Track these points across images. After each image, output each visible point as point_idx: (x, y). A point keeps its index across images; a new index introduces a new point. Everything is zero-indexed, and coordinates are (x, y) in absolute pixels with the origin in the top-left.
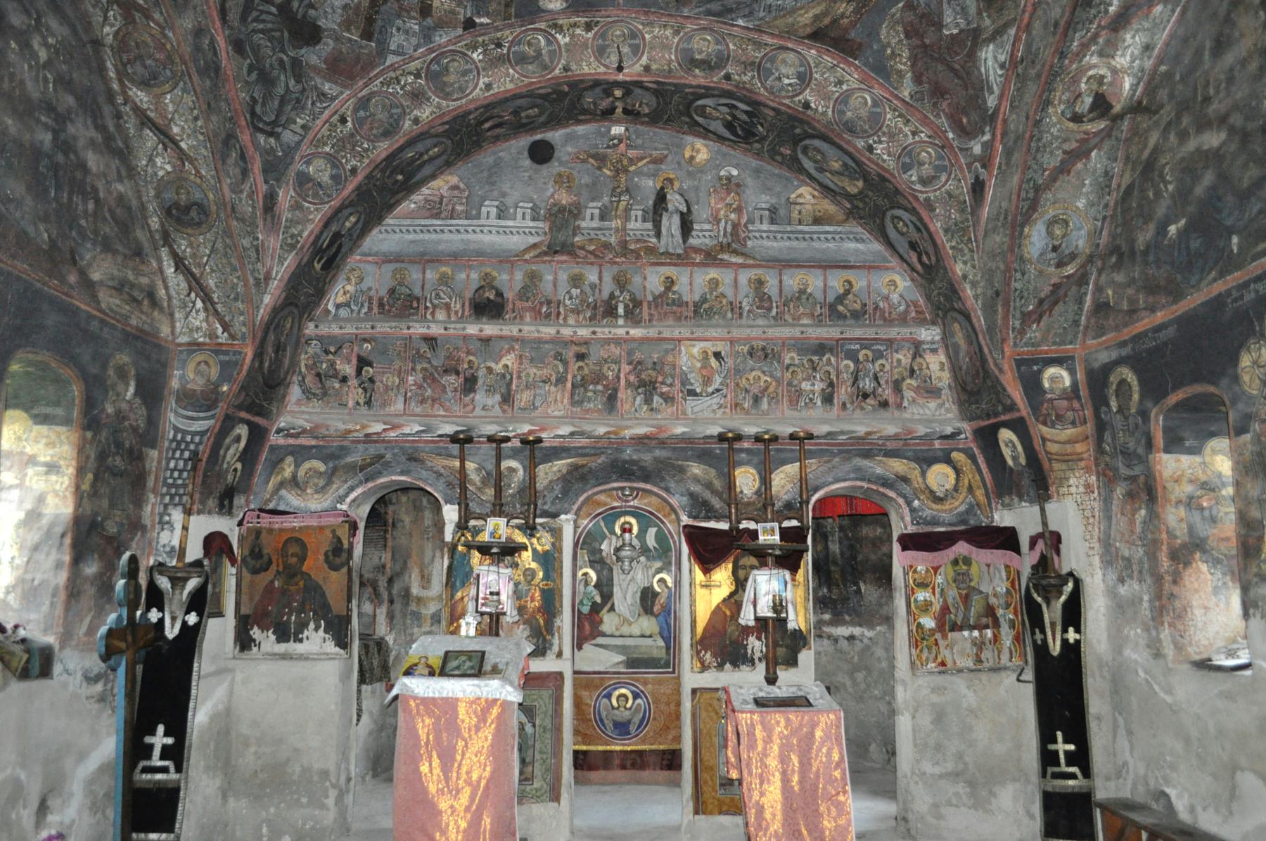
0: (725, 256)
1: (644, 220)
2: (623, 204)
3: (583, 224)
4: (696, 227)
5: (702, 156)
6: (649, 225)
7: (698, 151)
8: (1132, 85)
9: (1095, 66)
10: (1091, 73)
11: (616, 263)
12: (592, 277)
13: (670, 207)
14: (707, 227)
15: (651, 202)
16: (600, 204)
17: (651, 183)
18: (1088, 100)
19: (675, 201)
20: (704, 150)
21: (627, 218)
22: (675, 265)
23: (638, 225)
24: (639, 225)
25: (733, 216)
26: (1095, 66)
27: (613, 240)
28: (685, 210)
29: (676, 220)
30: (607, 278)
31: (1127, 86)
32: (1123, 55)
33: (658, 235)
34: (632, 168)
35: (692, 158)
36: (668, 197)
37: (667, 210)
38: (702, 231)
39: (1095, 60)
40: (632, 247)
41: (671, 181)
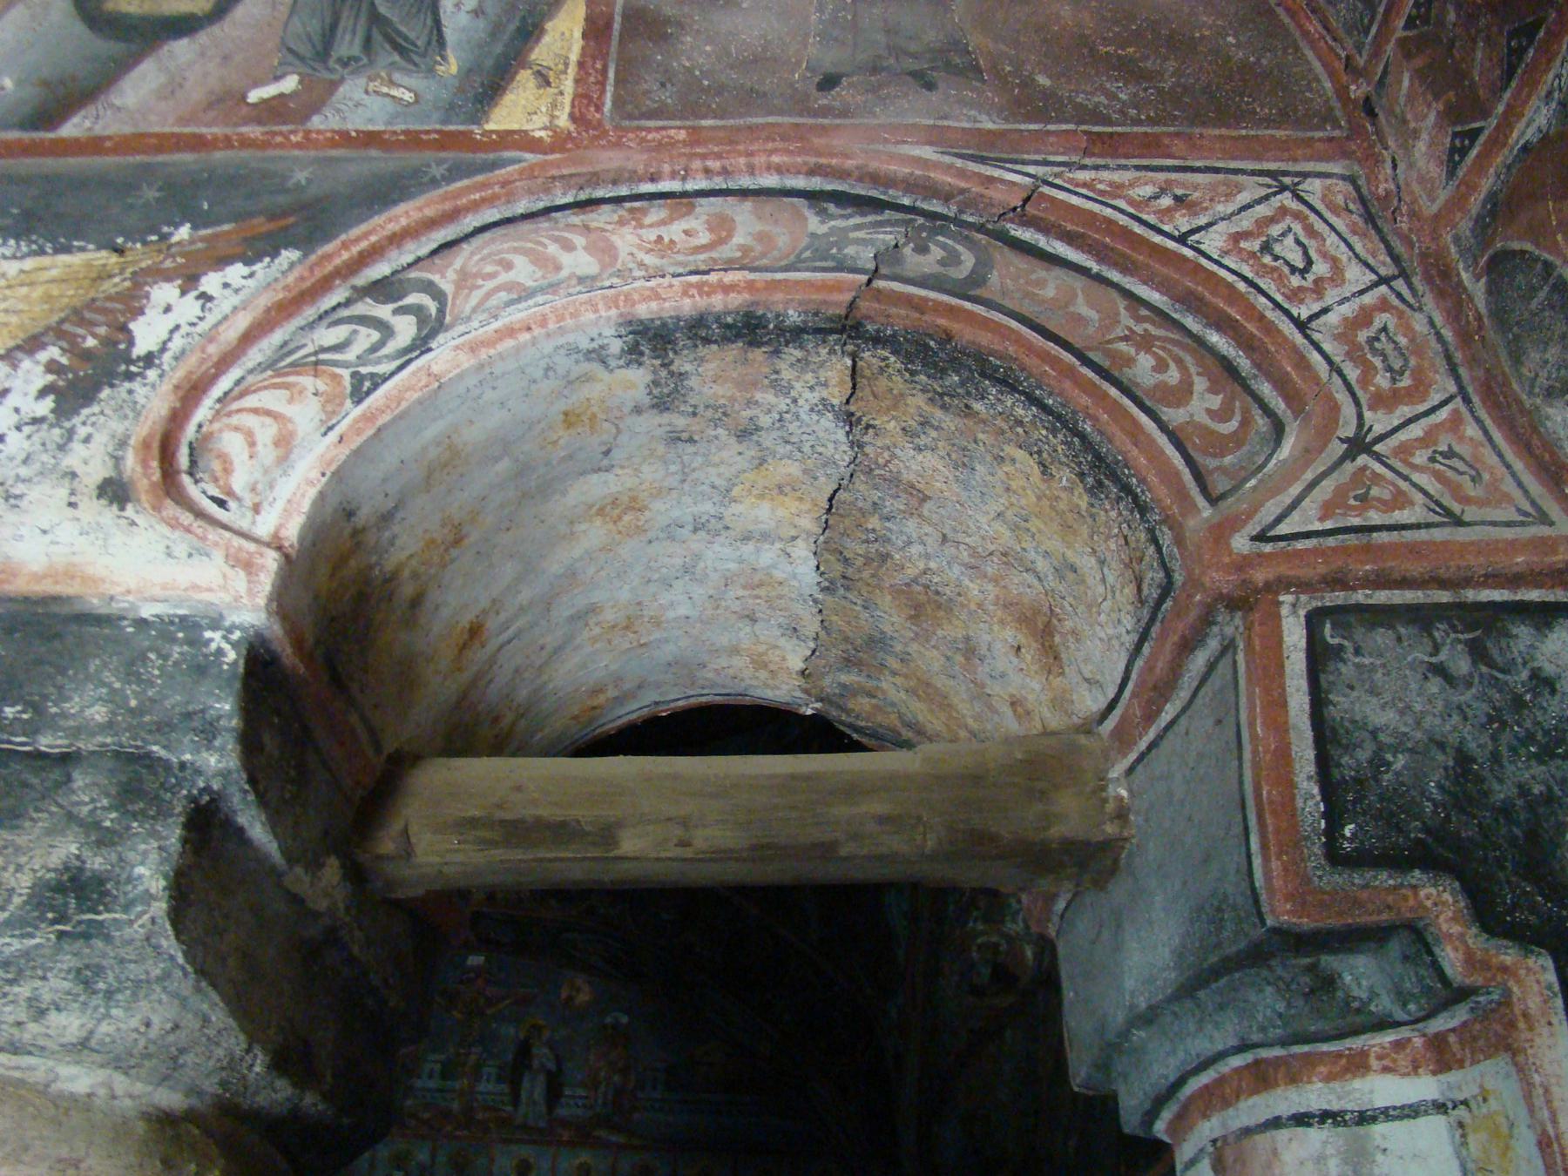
0: (602, 1133)
1: (499, 1080)
2: (473, 1057)
3: (419, 1084)
4: (567, 1092)
5: (583, 997)
6: (505, 1088)
7: (578, 990)
8: (1035, 954)
9: (983, 933)
10: (979, 941)
11: (456, 1138)
12: (423, 1156)
13: (536, 1064)
14: (581, 1092)
15: (510, 1057)
16: (443, 1057)
17: (512, 1031)
18: (986, 972)
19: (542, 1055)
20: (586, 988)
21: (476, 1075)
22: (535, 1142)
23: (488, 1087)
24: (490, 1087)
25: (616, 1078)
26: (983, 933)
27: (455, 1106)
28: (552, 1066)
29: (541, 1078)
30: (442, 1159)
31: (1029, 953)
32: (1014, 921)
33: (516, 1100)
34: (489, 1012)
35: (570, 998)
36: (535, 1051)
37: (529, 1067)
38: (573, 1097)
39: (980, 927)
40: (480, 1116)
41: (537, 1029)
